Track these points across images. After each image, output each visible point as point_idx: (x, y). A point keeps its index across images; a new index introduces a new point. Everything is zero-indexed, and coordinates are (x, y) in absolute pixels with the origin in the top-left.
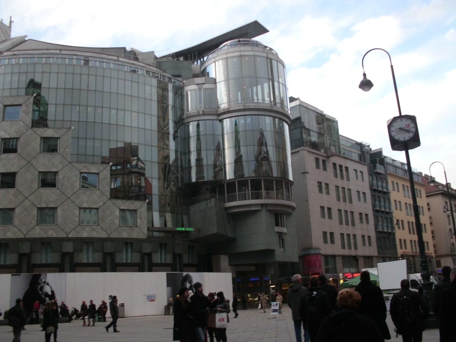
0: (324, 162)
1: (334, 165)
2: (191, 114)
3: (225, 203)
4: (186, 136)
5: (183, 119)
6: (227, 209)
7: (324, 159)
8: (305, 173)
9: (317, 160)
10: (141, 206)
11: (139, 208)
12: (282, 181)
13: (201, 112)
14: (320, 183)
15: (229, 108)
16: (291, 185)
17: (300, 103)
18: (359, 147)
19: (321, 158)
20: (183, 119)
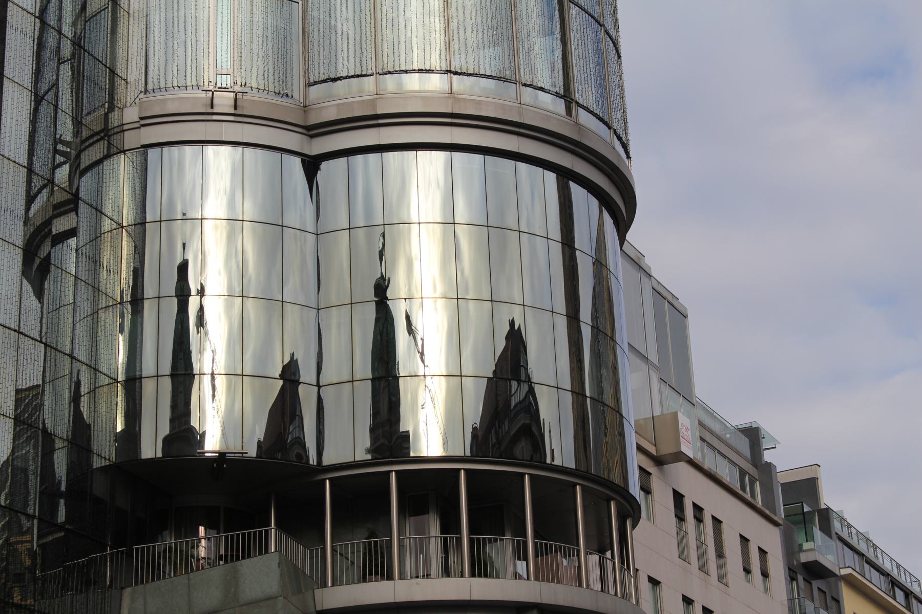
1: (678, 498)
2: (172, 108)
3: (325, 585)
5: (121, 129)
13: (224, 102)
15: (373, 102)
18: (744, 445)
20: (121, 129)
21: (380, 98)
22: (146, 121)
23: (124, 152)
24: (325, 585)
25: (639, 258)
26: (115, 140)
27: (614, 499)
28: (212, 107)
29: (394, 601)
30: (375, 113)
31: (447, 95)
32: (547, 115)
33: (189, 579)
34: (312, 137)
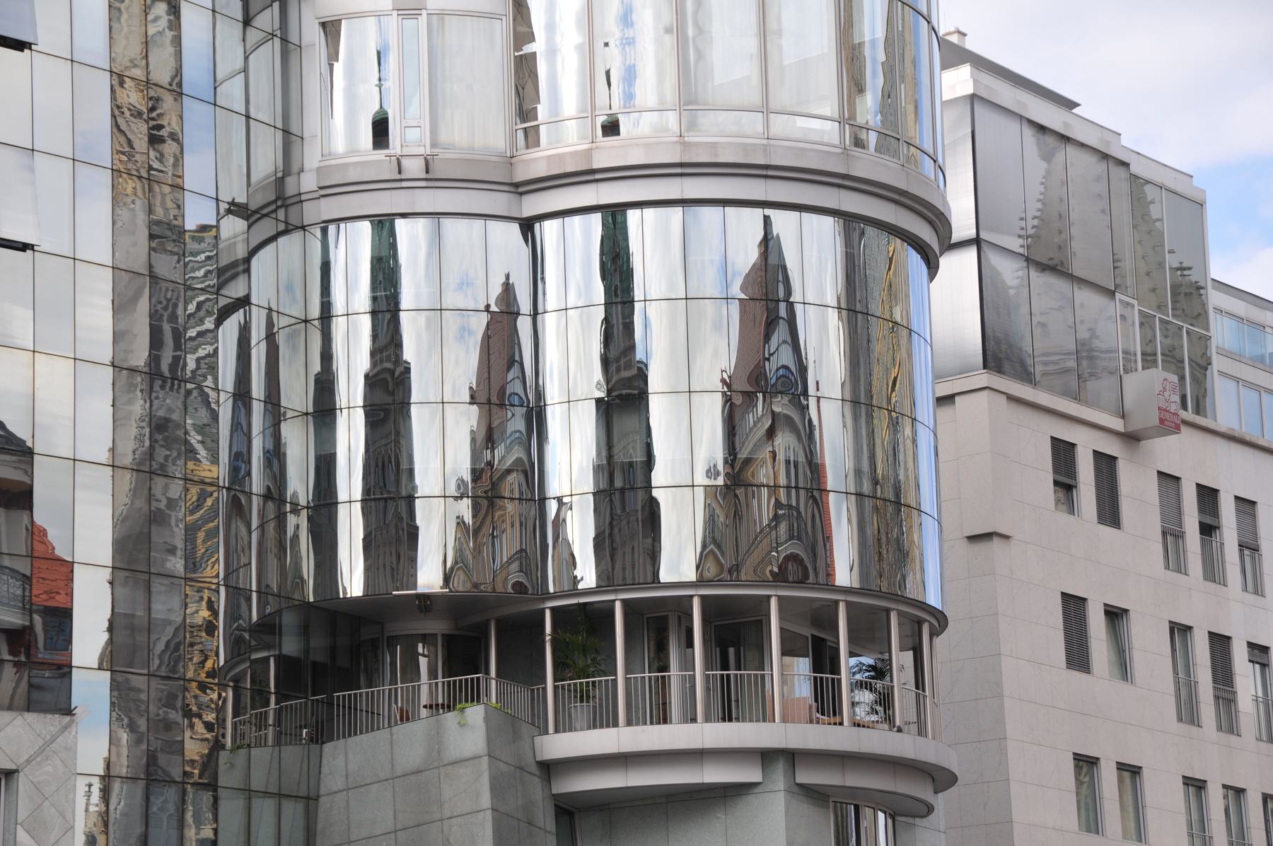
0: (1105, 464)
3: (547, 733)
4: (315, 311)
5: (299, 200)
6: (550, 769)
7: (1110, 447)
8: (987, 536)
9: (1063, 453)
10: (42, 750)
11: (28, 761)
12: (888, 611)
13: (414, 167)
14: (1073, 605)
16: (933, 634)
17: (976, 82)
19: (1086, 444)
20: (299, 200)
21: (597, 148)
22: (327, 191)
23: (303, 228)
24: (547, 733)
25: (1108, 143)
26: (292, 210)
27: (893, 609)
28: (400, 173)
29: (617, 752)
30: (590, 168)
31: (676, 139)
32: (802, 149)
33: (391, 734)
34: (521, 194)
